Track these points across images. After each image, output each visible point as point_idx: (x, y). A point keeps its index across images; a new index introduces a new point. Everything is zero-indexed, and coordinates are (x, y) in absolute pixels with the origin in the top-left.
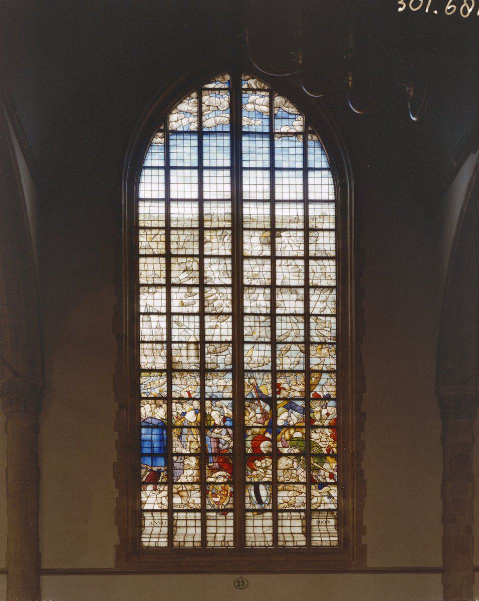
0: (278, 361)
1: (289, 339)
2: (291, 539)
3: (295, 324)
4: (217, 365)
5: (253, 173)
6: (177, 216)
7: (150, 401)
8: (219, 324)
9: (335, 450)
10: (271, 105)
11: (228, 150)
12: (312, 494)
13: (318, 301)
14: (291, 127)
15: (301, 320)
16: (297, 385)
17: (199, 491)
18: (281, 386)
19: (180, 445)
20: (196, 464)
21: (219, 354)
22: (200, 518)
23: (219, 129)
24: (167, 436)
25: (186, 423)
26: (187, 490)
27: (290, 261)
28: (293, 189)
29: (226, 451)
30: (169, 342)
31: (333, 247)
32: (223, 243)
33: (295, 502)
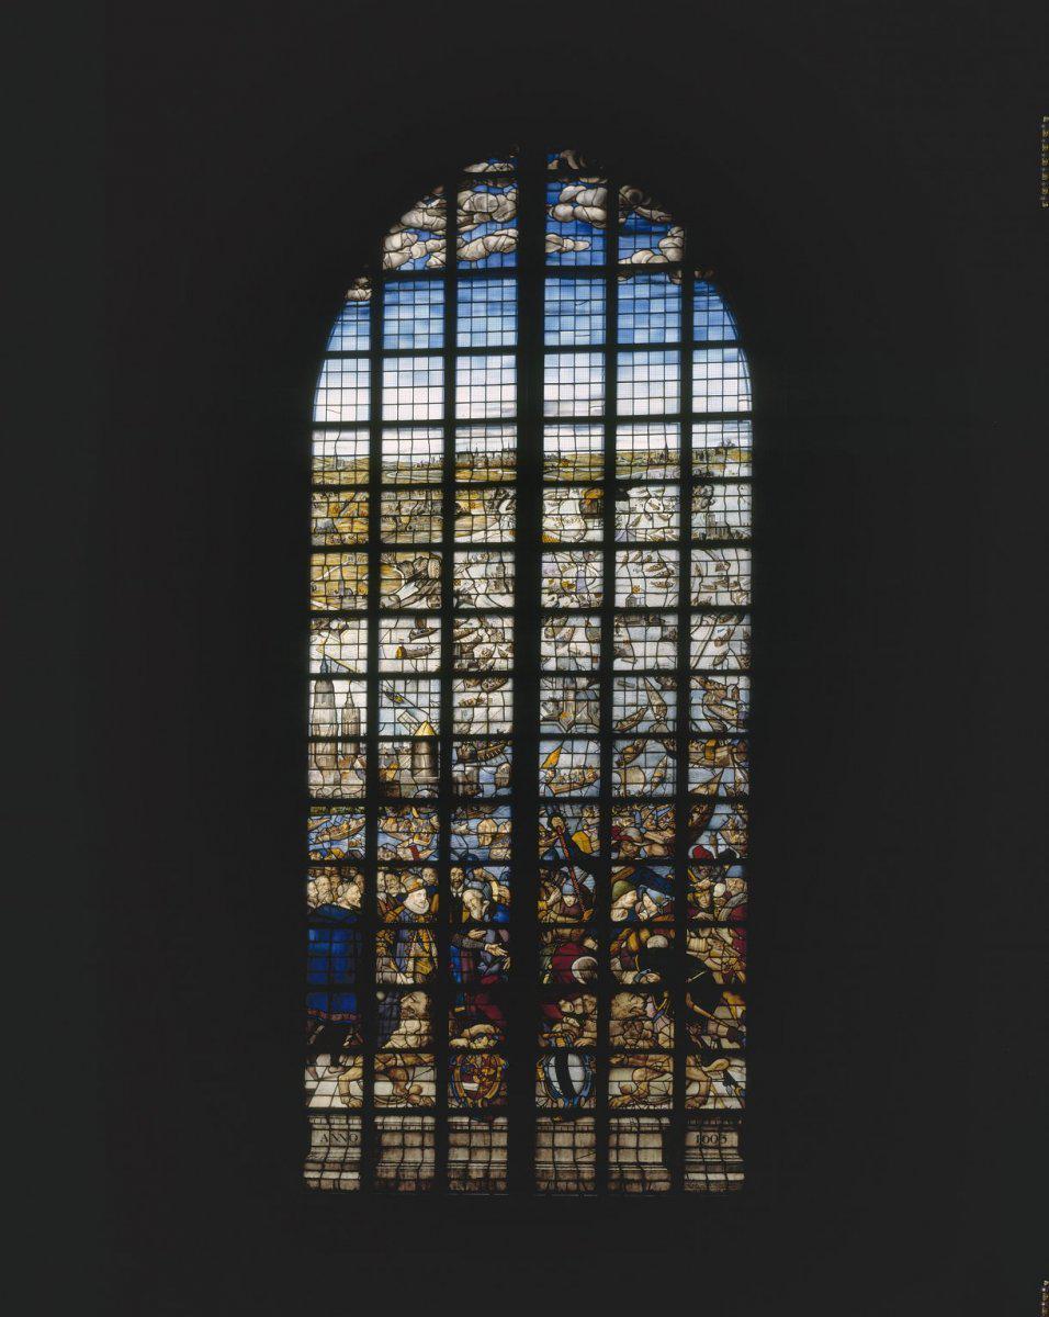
0: (616, 778)
1: (643, 728)
2: (636, 1177)
3: (655, 695)
4: (478, 788)
5: (566, 359)
6: (395, 459)
8: (484, 696)
9: (742, 976)
10: (609, 204)
11: (511, 310)
12: (688, 1075)
13: (710, 640)
14: (656, 251)
15: (669, 684)
16: (658, 829)
17: (433, 1068)
18: (623, 833)
20: (427, 1008)
21: (484, 763)
23: (494, 262)
26: (405, 1067)
27: (646, 554)
28: (657, 390)
29: (496, 978)
30: (373, 737)
31: (746, 518)
32: (498, 517)
33: (649, 1094)
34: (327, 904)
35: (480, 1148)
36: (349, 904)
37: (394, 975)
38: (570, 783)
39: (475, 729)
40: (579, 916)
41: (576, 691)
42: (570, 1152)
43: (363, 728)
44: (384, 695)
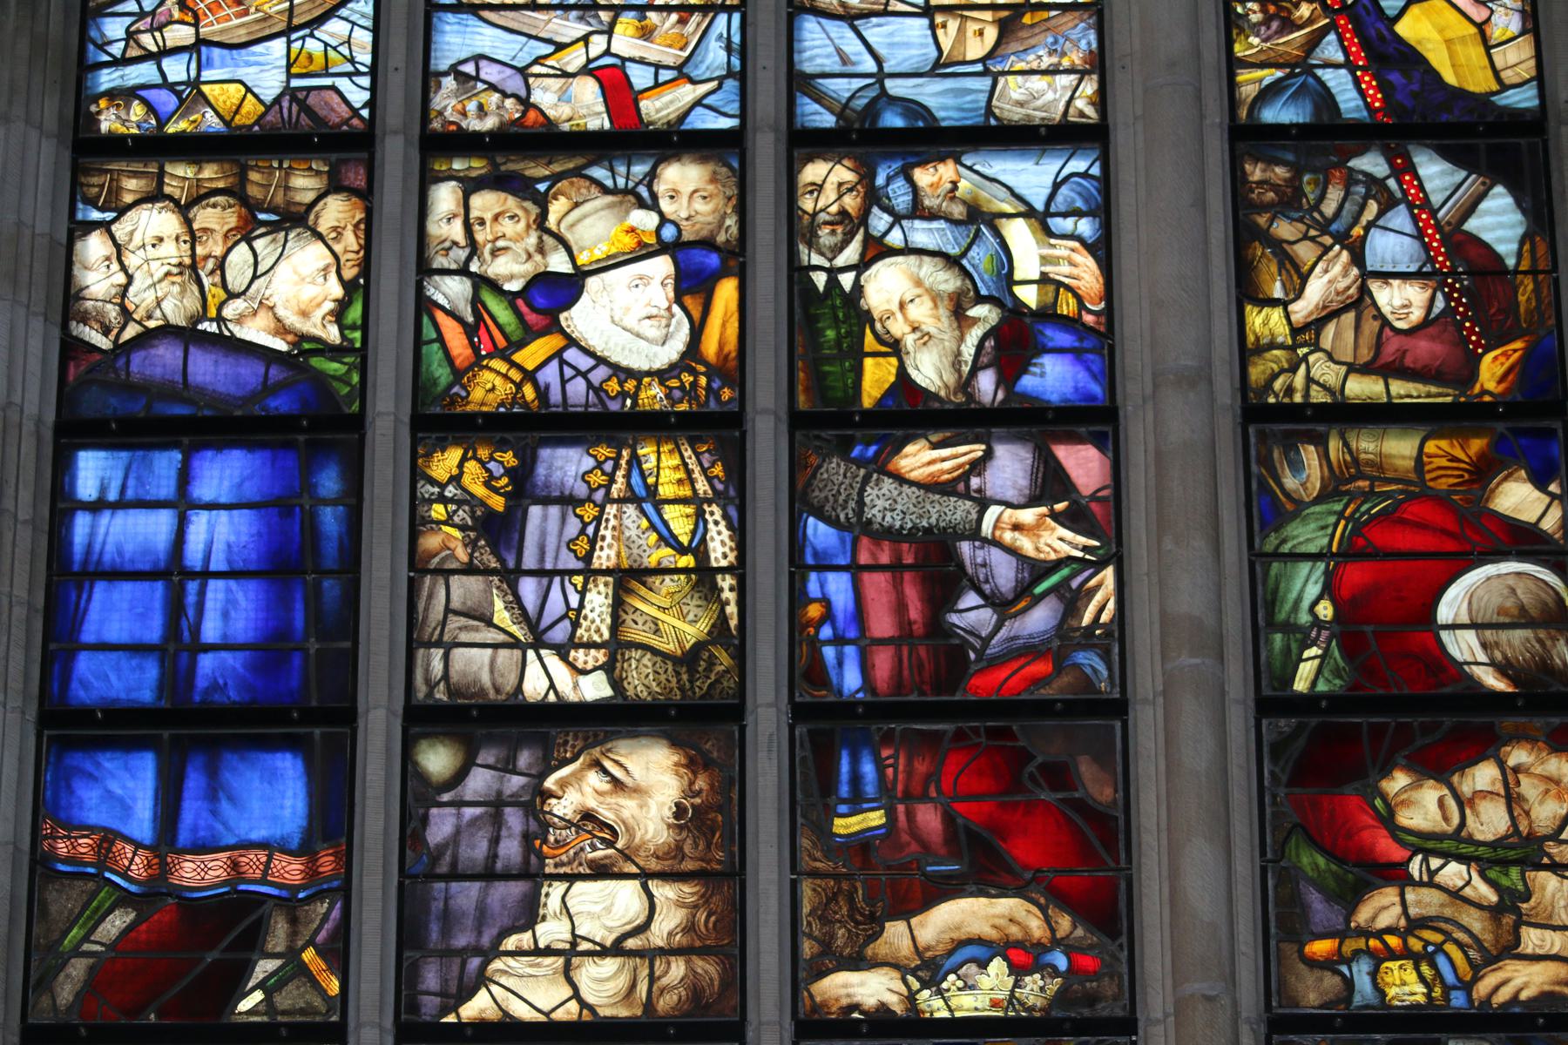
7: (182, 170)
19: (502, 616)
25: (577, 388)
29: (1041, 667)
34: (168, 330)
36: (281, 329)
37: (503, 654)
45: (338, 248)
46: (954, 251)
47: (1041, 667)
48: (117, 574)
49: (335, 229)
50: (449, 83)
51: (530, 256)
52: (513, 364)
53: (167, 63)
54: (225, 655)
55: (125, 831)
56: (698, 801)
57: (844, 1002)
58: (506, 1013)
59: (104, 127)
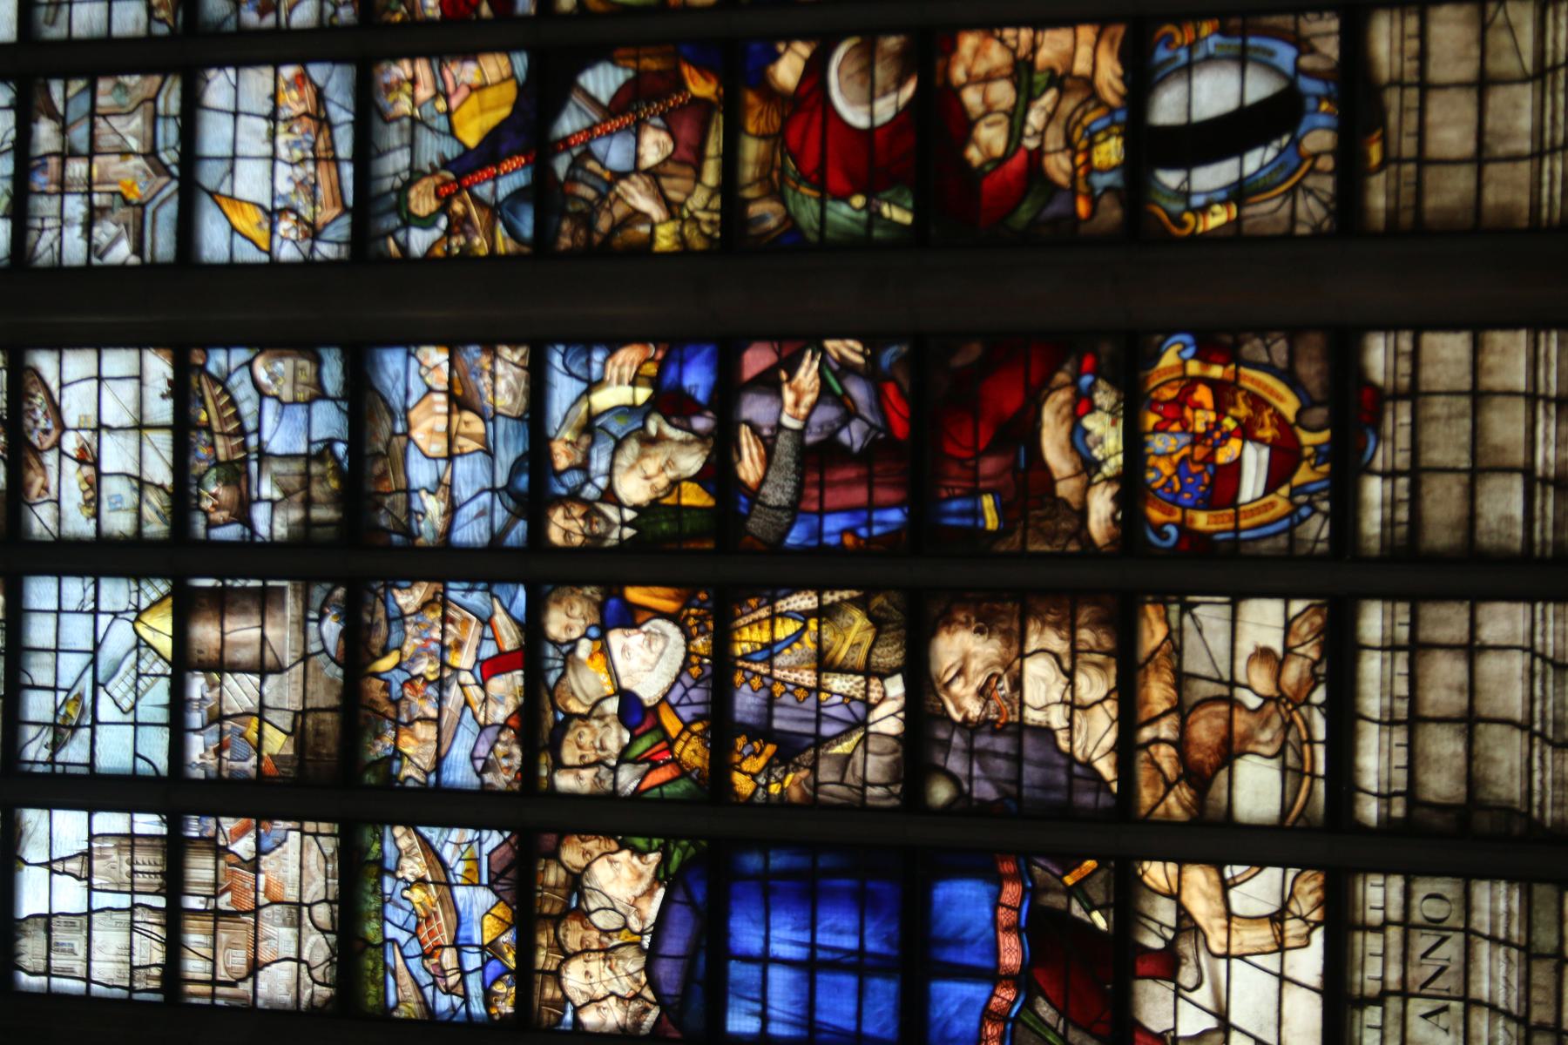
4: (320, 457)
7: (544, 959)
8: (70, 443)
17: (1187, 608)
19: (843, 748)
20: (984, 627)
21: (253, 441)
22: (1402, 609)
24: (781, 844)
25: (696, 695)
26: (1182, 710)
29: (891, 390)
34: (648, 969)
35: (1477, 434)
36: (649, 892)
37: (872, 746)
38: (316, 160)
39: (159, 471)
40: (702, 106)
41: (67, 154)
42: (1498, 98)
43: (149, 824)
44: (60, 757)
45: (597, 853)
46: (611, 443)
47: (891, 390)
48: (810, 1005)
49: (584, 855)
50: (488, 777)
51: (606, 725)
52: (678, 737)
53: (468, 968)
54: (868, 932)
55: (982, 1003)
56: (973, 619)
57: (1110, 524)
58: (1112, 749)
59: (509, 1010)
